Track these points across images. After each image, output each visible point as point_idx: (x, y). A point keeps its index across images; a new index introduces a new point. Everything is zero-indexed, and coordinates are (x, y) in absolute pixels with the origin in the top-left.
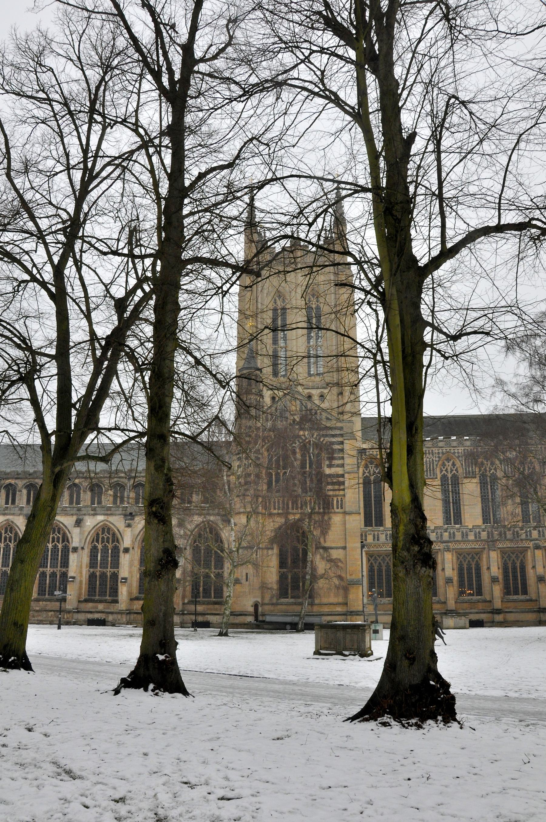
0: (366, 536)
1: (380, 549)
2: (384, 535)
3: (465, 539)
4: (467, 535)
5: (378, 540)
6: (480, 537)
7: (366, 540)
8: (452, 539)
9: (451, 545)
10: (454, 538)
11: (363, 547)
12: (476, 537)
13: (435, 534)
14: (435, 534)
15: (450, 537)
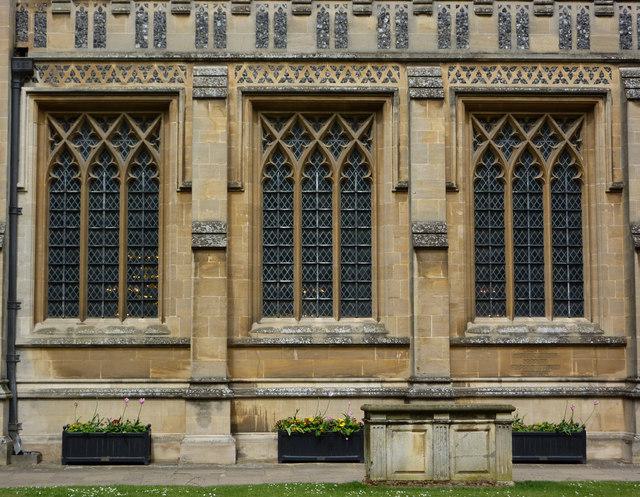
0: (41, 24)
1: (104, 86)
2: (129, 23)
3: (514, 50)
4: (525, 30)
5: (99, 42)
6: (585, 44)
7: (41, 42)
8: (453, 51)
9: (449, 79)
10: (462, 41)
11: (21, 75)
12: (565, 41)
13: (372, 21)
14: (372, 21)
15: (443, 39)
